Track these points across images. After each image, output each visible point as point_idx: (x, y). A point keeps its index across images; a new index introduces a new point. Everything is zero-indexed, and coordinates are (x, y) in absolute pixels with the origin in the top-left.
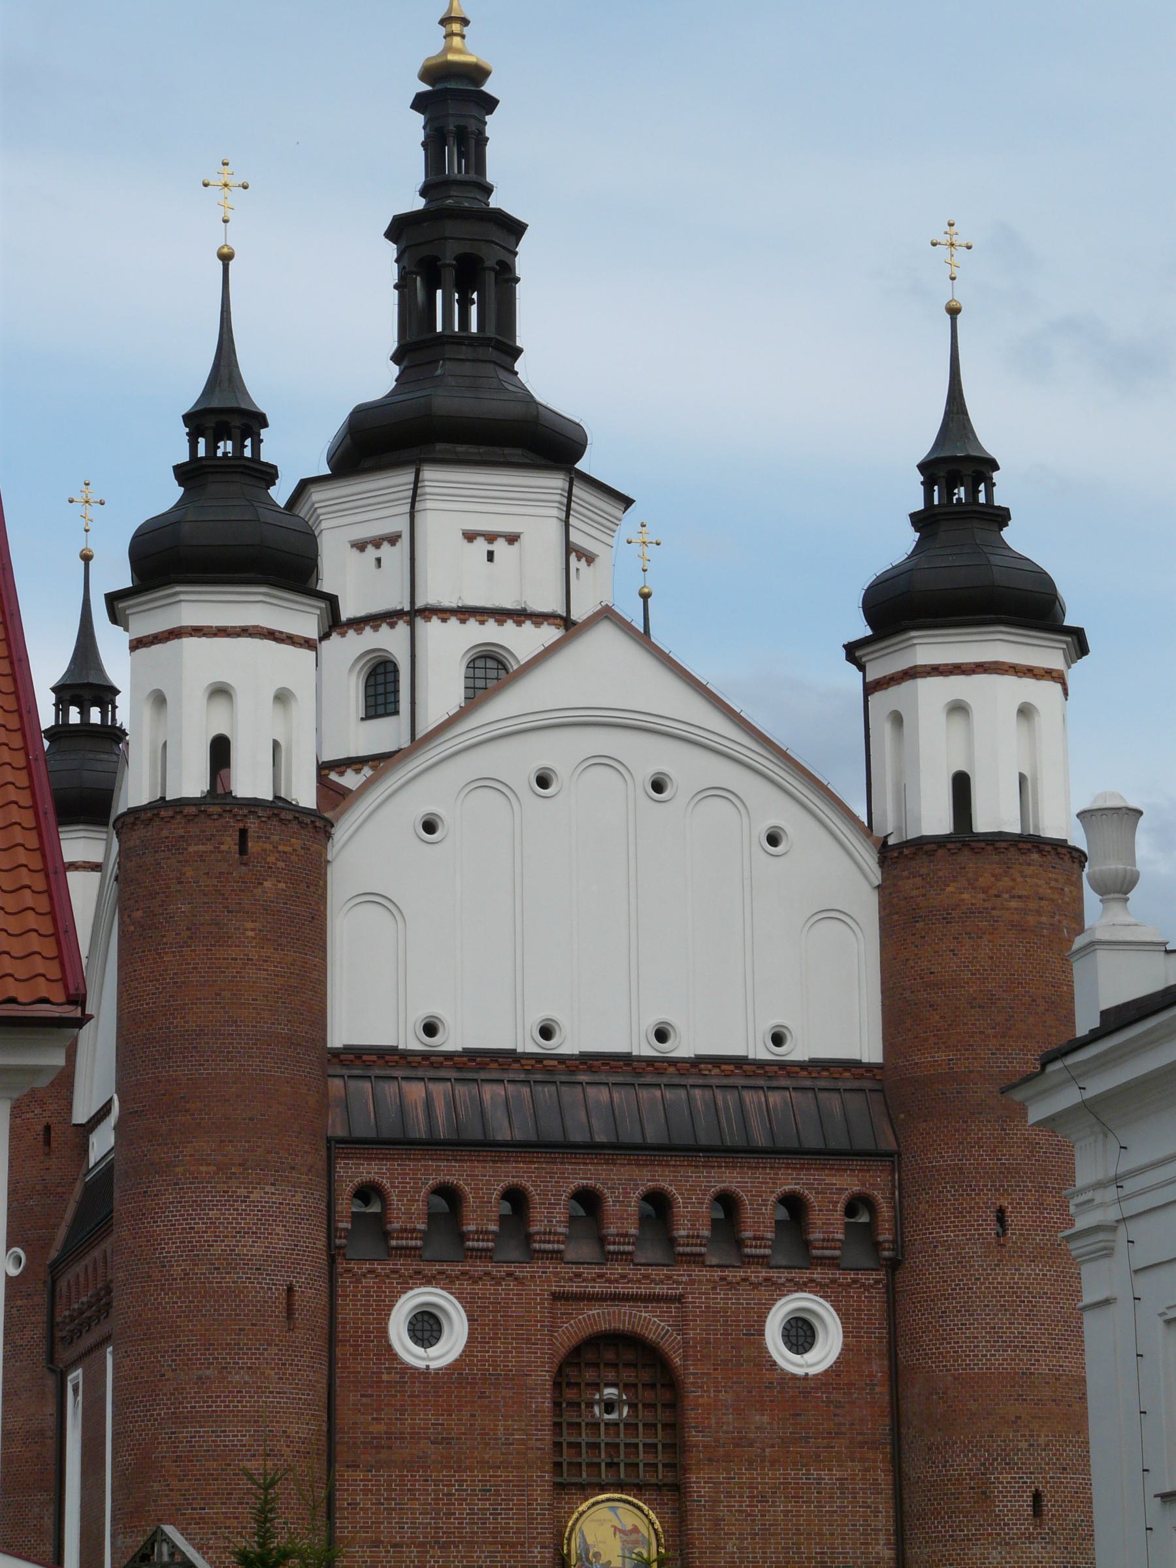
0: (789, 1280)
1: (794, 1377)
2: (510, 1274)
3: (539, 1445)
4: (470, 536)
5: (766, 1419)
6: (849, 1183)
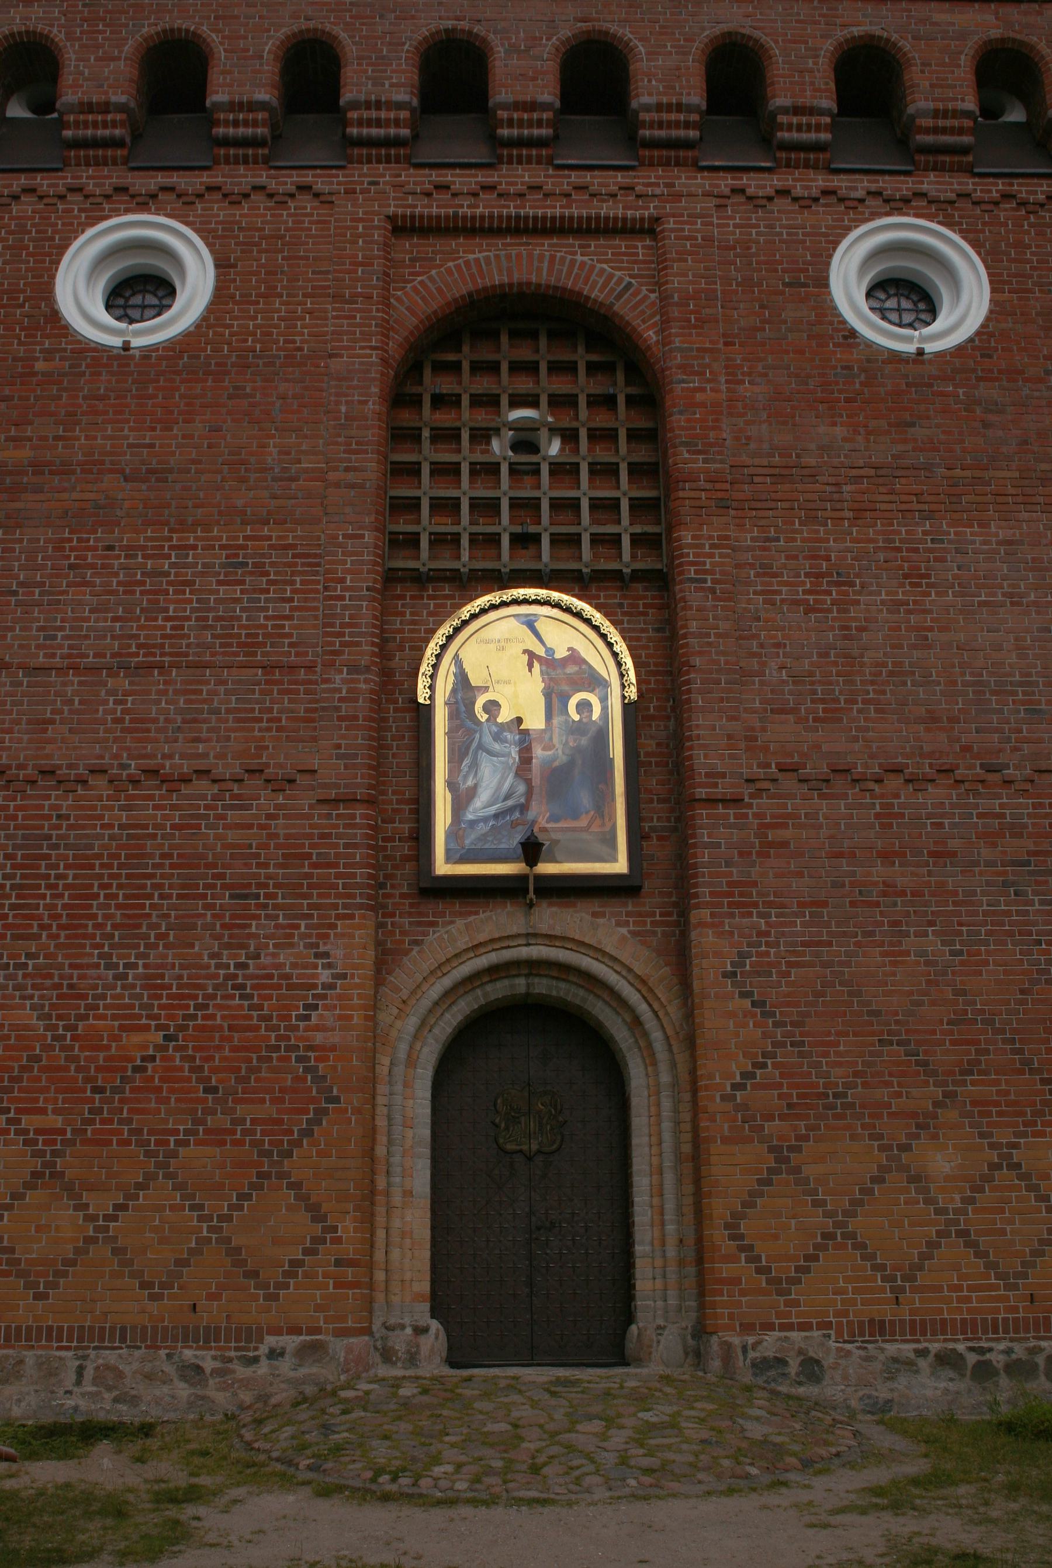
0: (878, 194)
2: (304, 188)
3: (351, 477)
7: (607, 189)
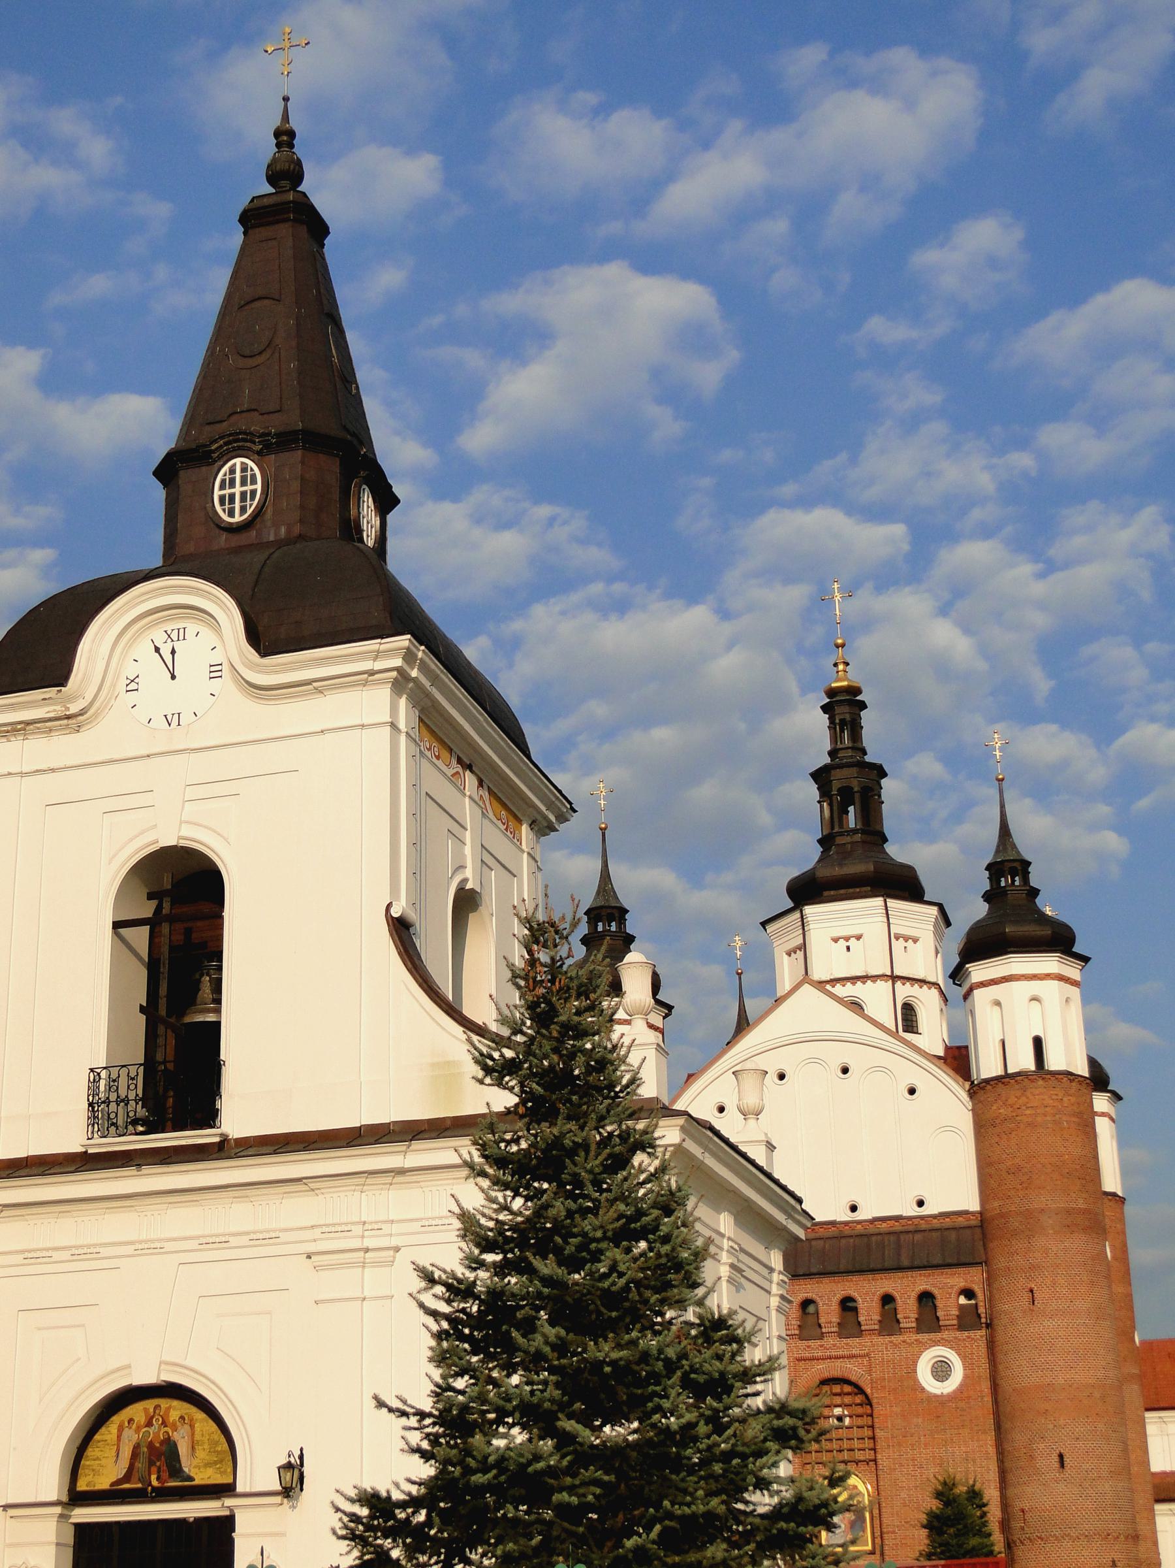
1: (936, 1396)
4: (836, 940)
5: (920, 1420)
6: (957, 1279)
7: (855, 1345)
